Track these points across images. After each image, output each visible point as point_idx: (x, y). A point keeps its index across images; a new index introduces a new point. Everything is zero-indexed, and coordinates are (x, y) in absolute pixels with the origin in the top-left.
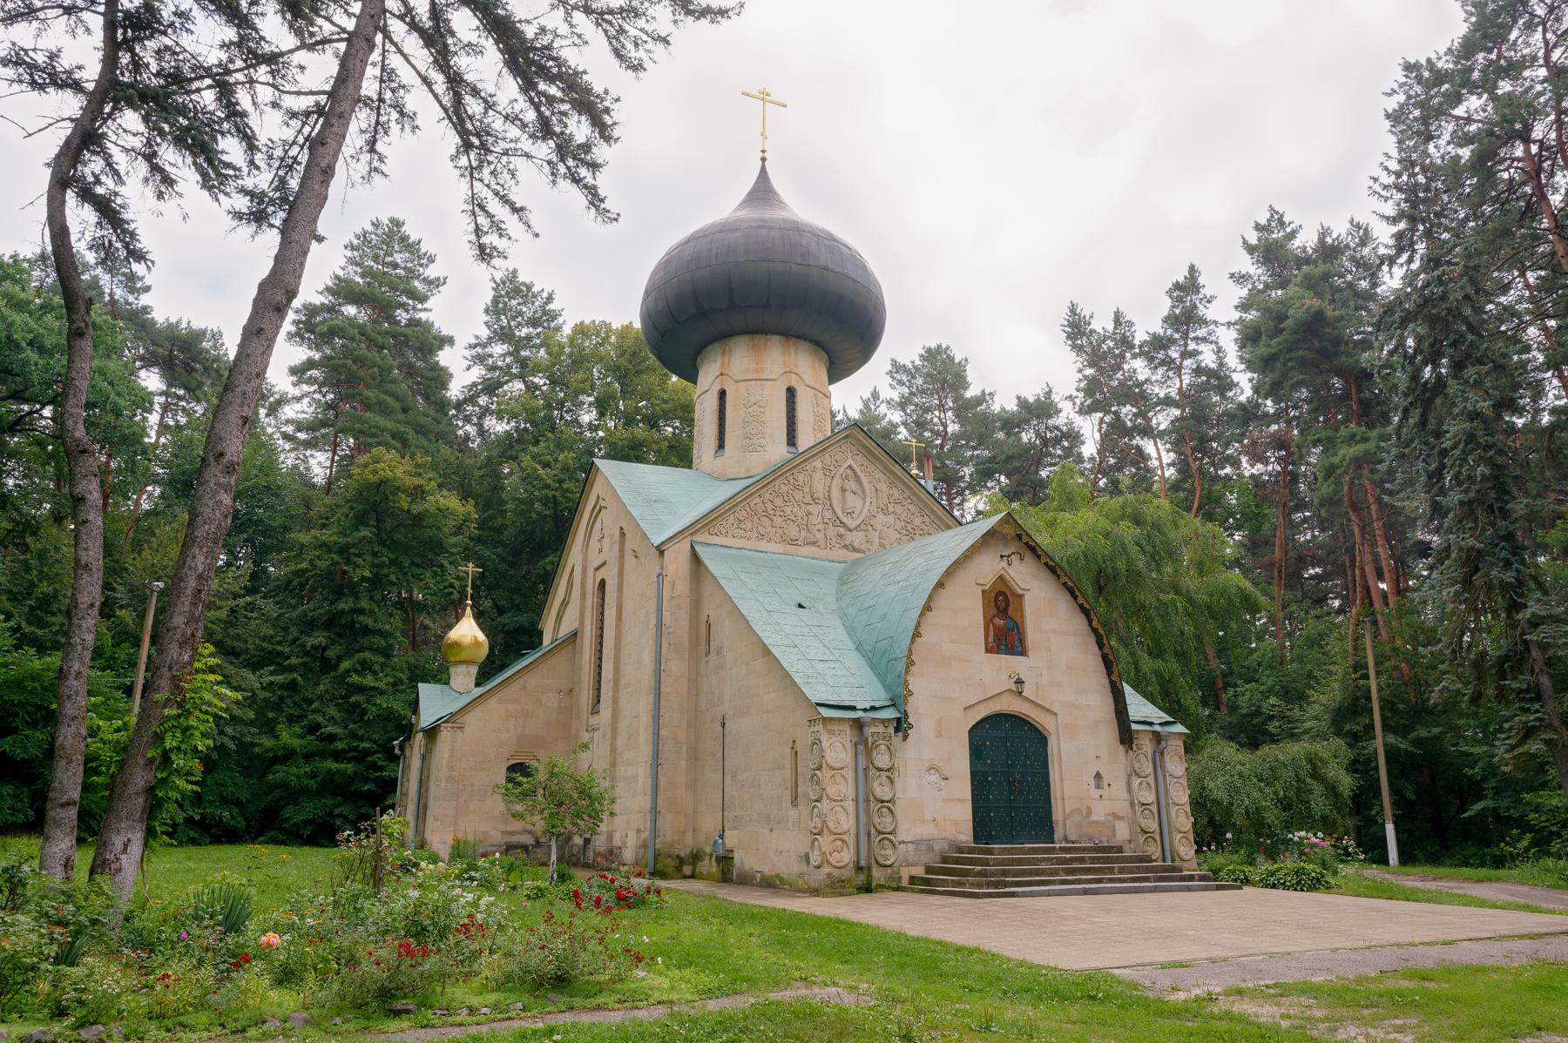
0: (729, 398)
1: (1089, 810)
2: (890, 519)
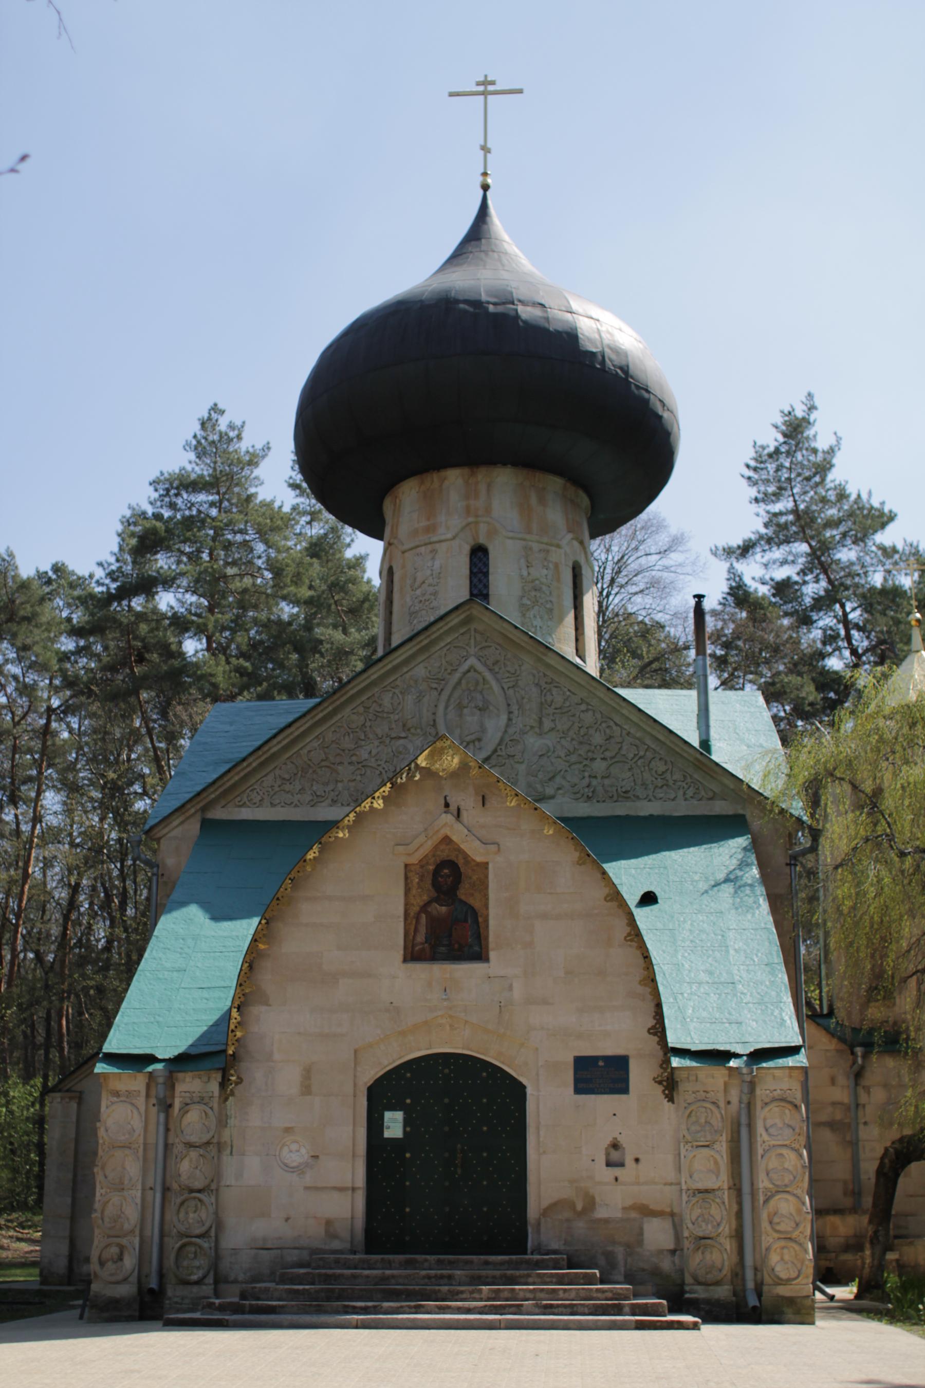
0: (396, 578)
1: (591, 1204)
2: (549, 741)
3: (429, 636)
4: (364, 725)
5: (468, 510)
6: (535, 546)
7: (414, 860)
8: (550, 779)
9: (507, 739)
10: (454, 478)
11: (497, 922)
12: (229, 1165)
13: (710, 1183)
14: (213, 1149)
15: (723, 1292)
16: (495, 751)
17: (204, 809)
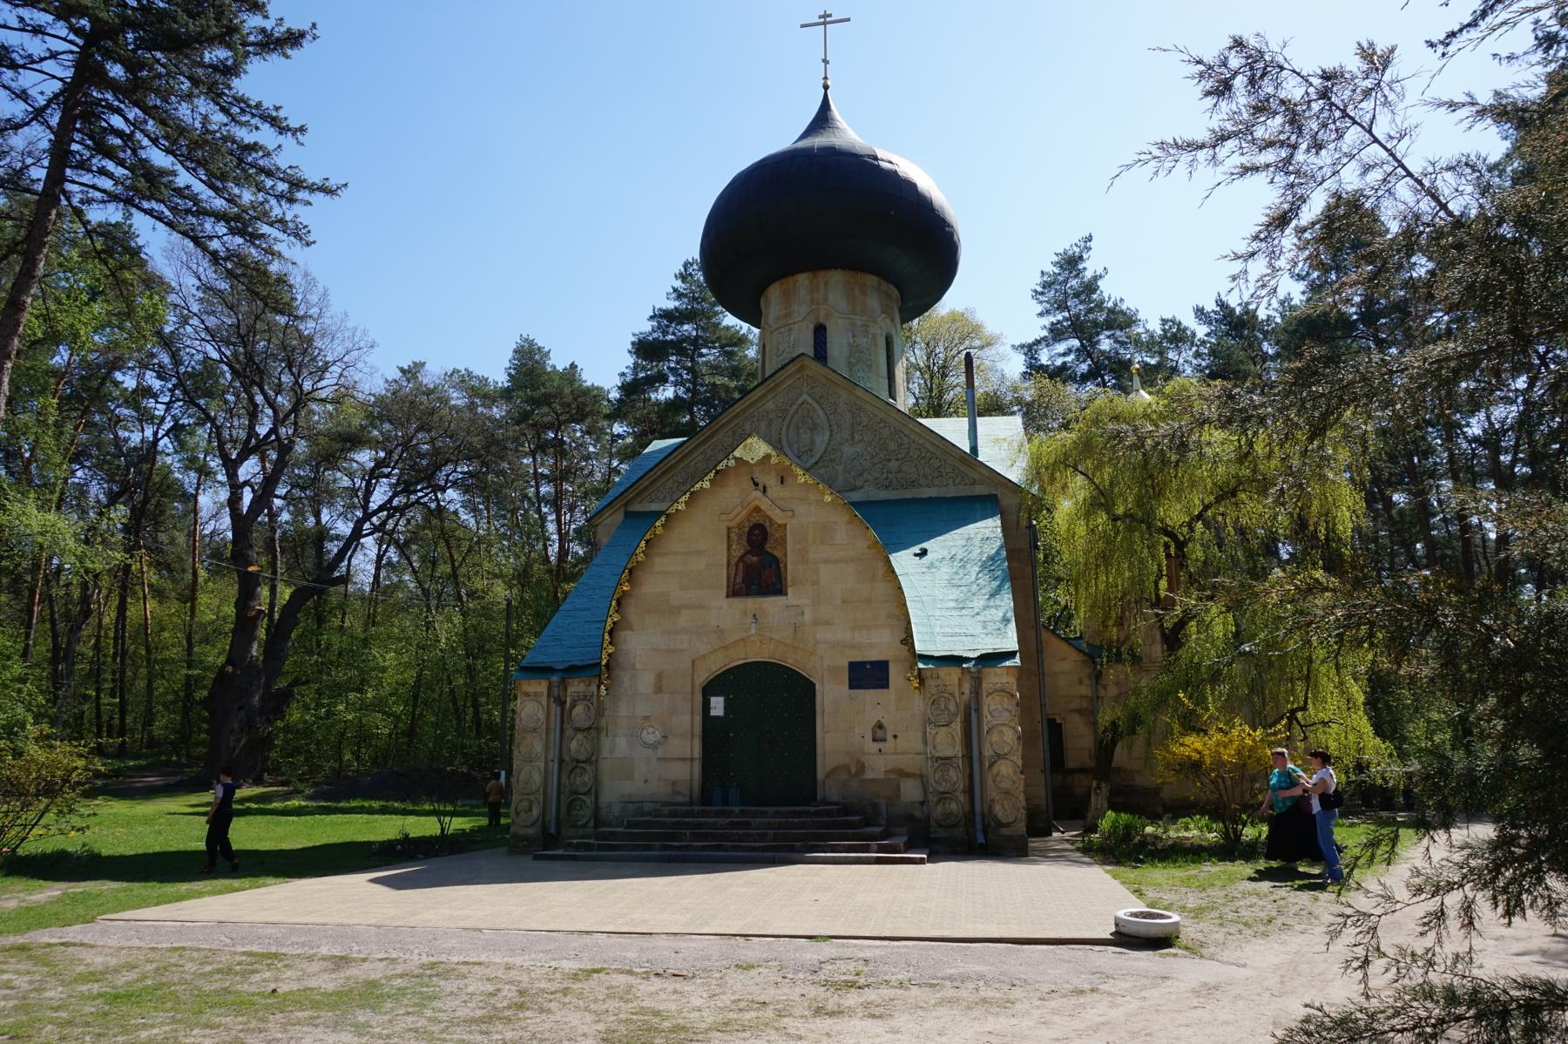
1: (862, 768)
5: (812, 301)
6: (859, 323)
7: (733, 524)
10: (803, 279)
11: (792, 568)
12: (606, 743)
13: (949, 753)
14: (593, 733)
15: (959, 833)
17: (626, 505)
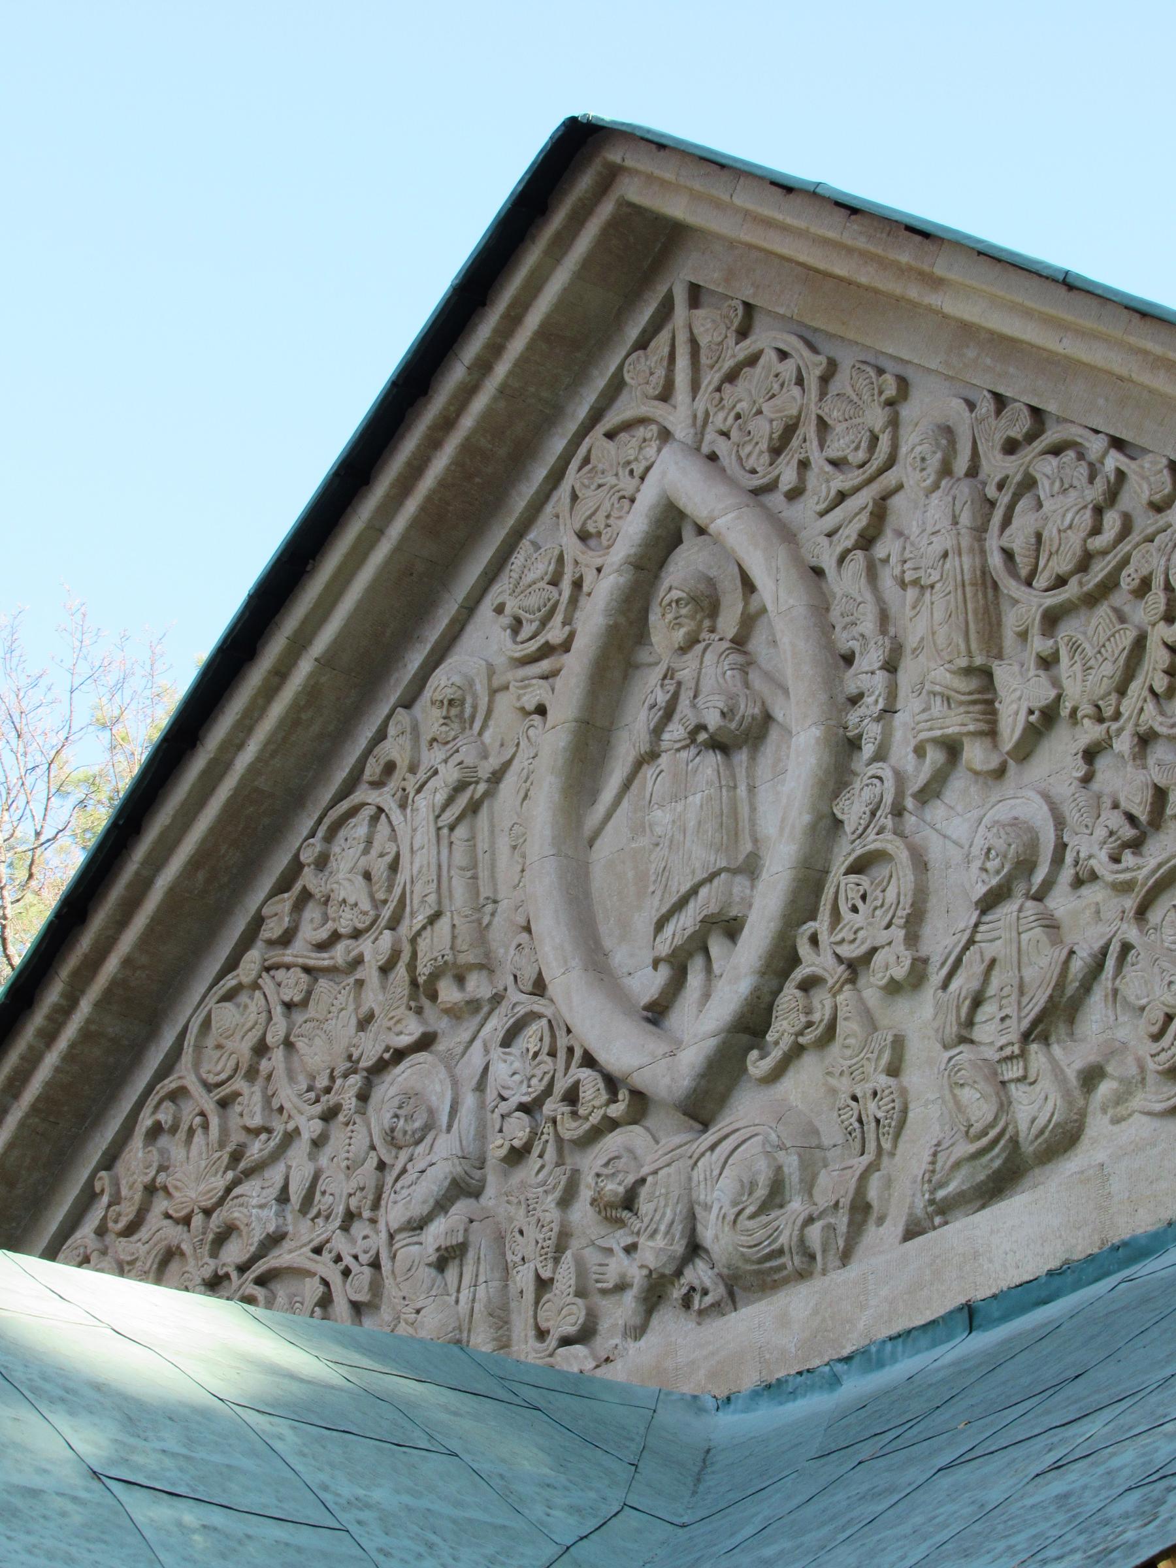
3: (447, 423)
4: (261, 1049)
8: (1039, 1031)
9: (844, 853)
16: (782, 960)
